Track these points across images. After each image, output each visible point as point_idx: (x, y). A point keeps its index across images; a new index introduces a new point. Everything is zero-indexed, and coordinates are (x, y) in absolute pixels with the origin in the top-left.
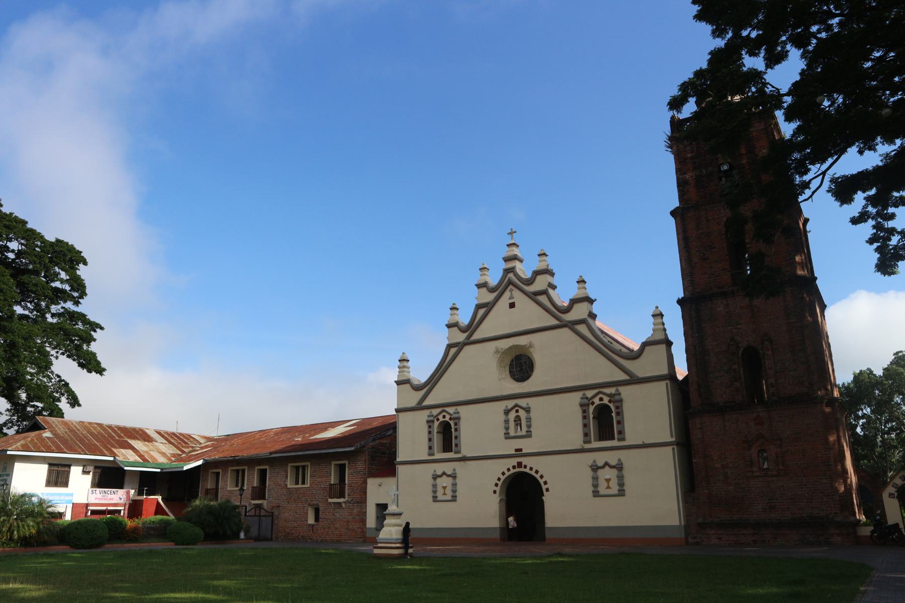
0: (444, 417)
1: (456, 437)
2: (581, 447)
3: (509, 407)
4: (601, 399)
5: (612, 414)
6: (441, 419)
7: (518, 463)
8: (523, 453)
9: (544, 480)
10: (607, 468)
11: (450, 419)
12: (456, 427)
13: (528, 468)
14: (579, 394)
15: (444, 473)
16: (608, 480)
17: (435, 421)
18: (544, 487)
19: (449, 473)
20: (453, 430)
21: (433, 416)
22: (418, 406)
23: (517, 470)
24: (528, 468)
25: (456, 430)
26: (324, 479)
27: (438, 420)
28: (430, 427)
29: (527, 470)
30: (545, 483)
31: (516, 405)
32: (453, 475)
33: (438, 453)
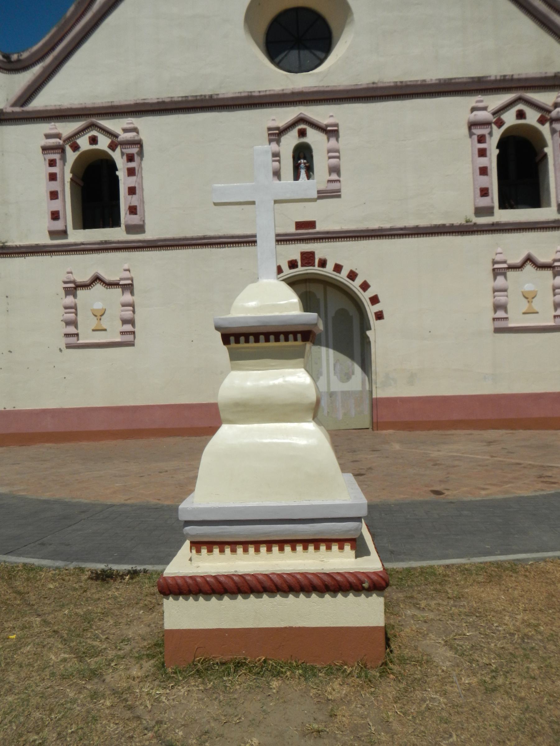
0: (94, 140)
1: (132, 191)
2: (463, 222)
3: (281, 123)
4: (521, 115)
5: (546, 150)
6: (84, 143)
7: (303, 254)
8: (318, 233)
9: (370, 293)
10: (529, 267)
11: (113, 147)
12: (131, 165)
13: (330, 267)
14: (472, 101)
15: (97, 279)
16: (529, 297)
17: (68, 149)
18: (371, 310)
19: (108, 277)
20: (121, 174)
21: (58, 136)
22: (17, 109)
23: (300, 270)
24: (330, 267)
25: (131, 172)
27: (75, 147)
28: (52, 163)
29: (329, 270)
30: (375, 300)
31: (301, 120)
32: (122, 282)
33: (75, 227)
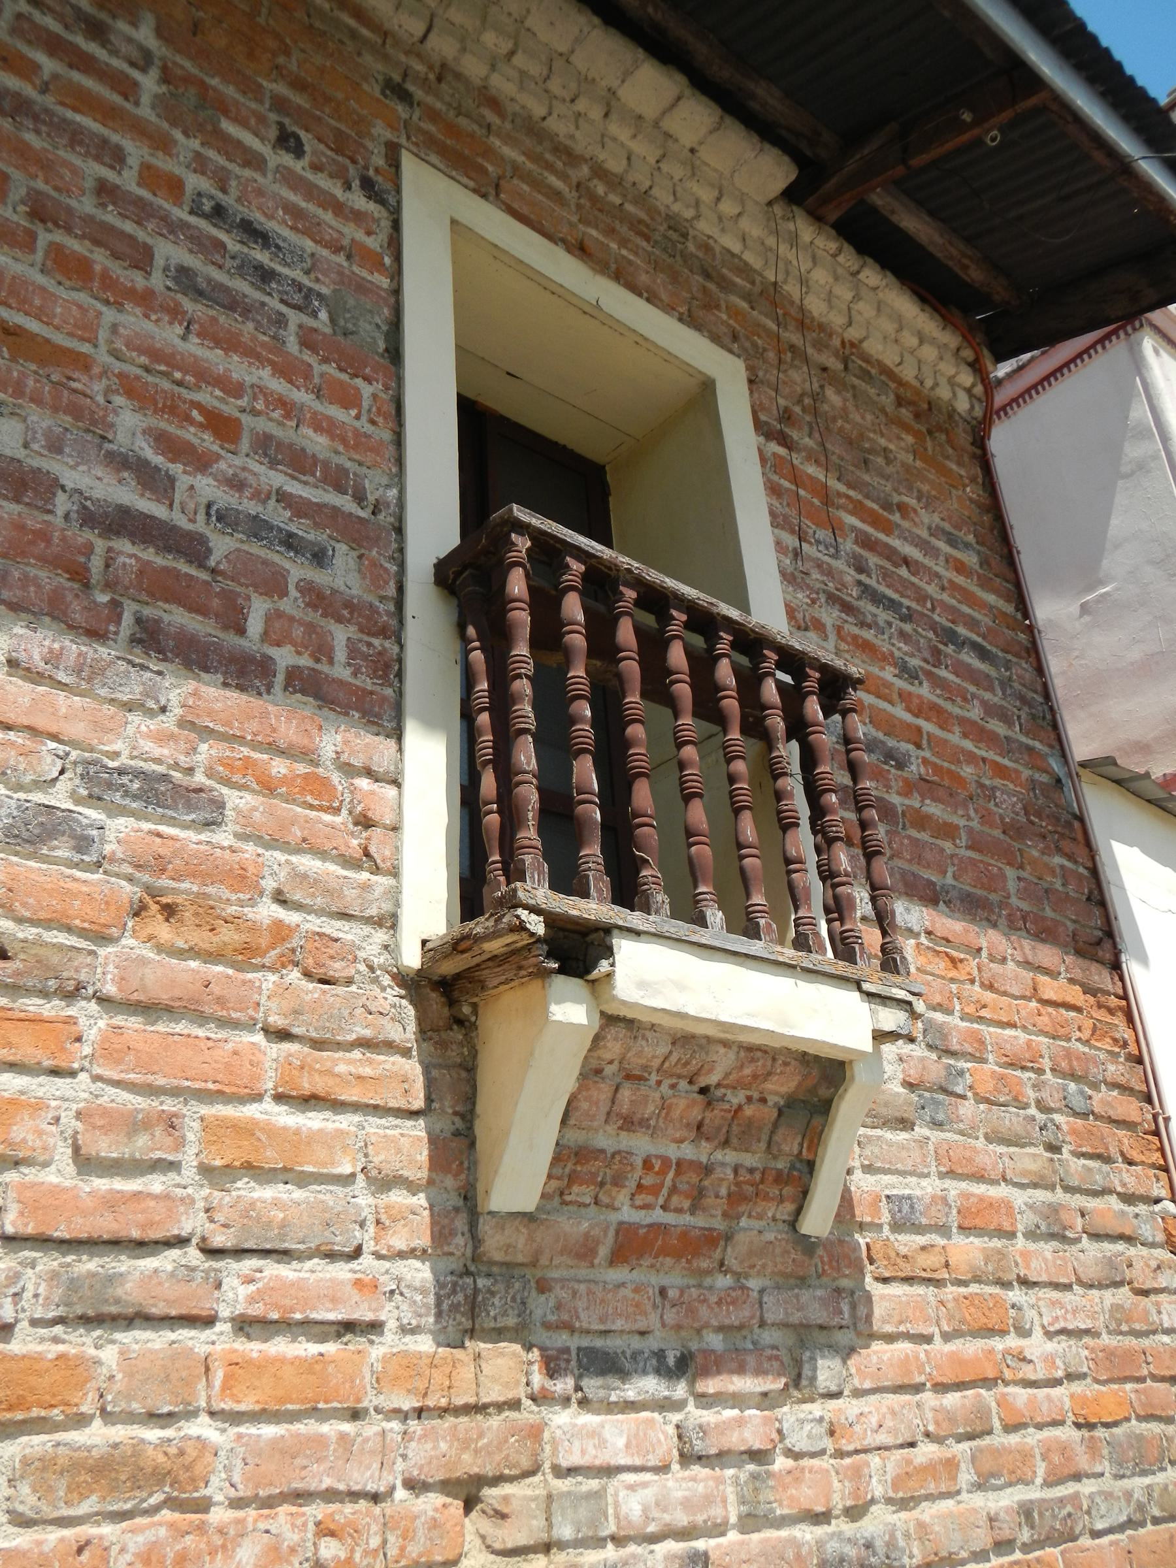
26: (133, 321)
